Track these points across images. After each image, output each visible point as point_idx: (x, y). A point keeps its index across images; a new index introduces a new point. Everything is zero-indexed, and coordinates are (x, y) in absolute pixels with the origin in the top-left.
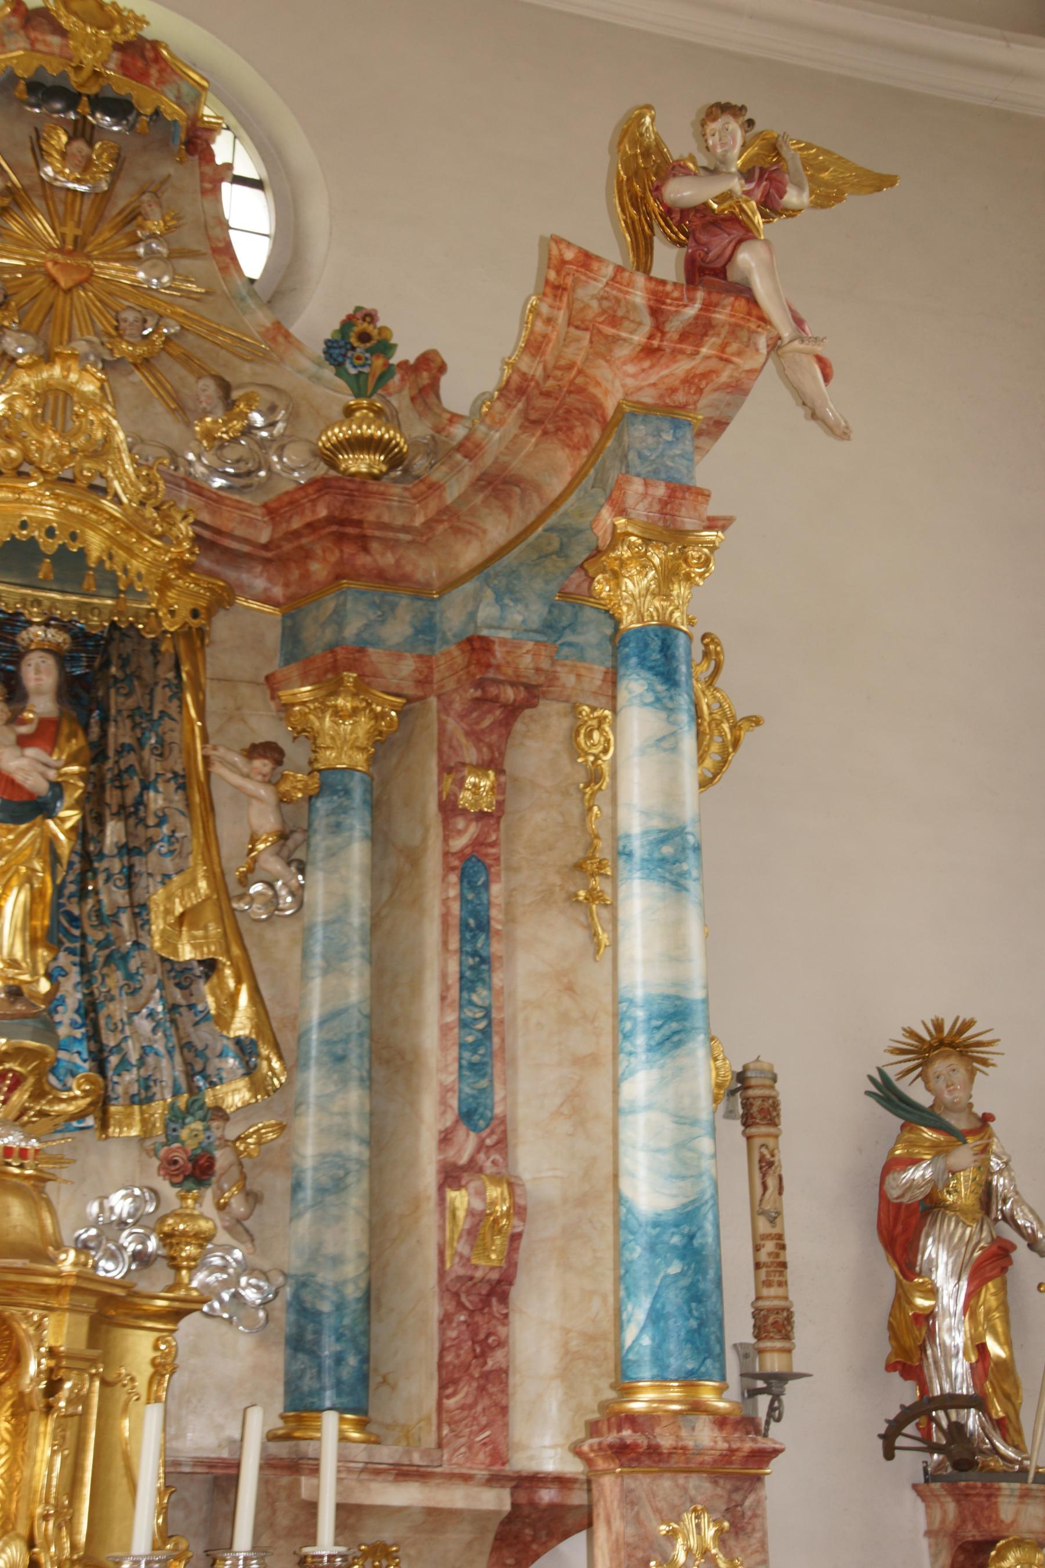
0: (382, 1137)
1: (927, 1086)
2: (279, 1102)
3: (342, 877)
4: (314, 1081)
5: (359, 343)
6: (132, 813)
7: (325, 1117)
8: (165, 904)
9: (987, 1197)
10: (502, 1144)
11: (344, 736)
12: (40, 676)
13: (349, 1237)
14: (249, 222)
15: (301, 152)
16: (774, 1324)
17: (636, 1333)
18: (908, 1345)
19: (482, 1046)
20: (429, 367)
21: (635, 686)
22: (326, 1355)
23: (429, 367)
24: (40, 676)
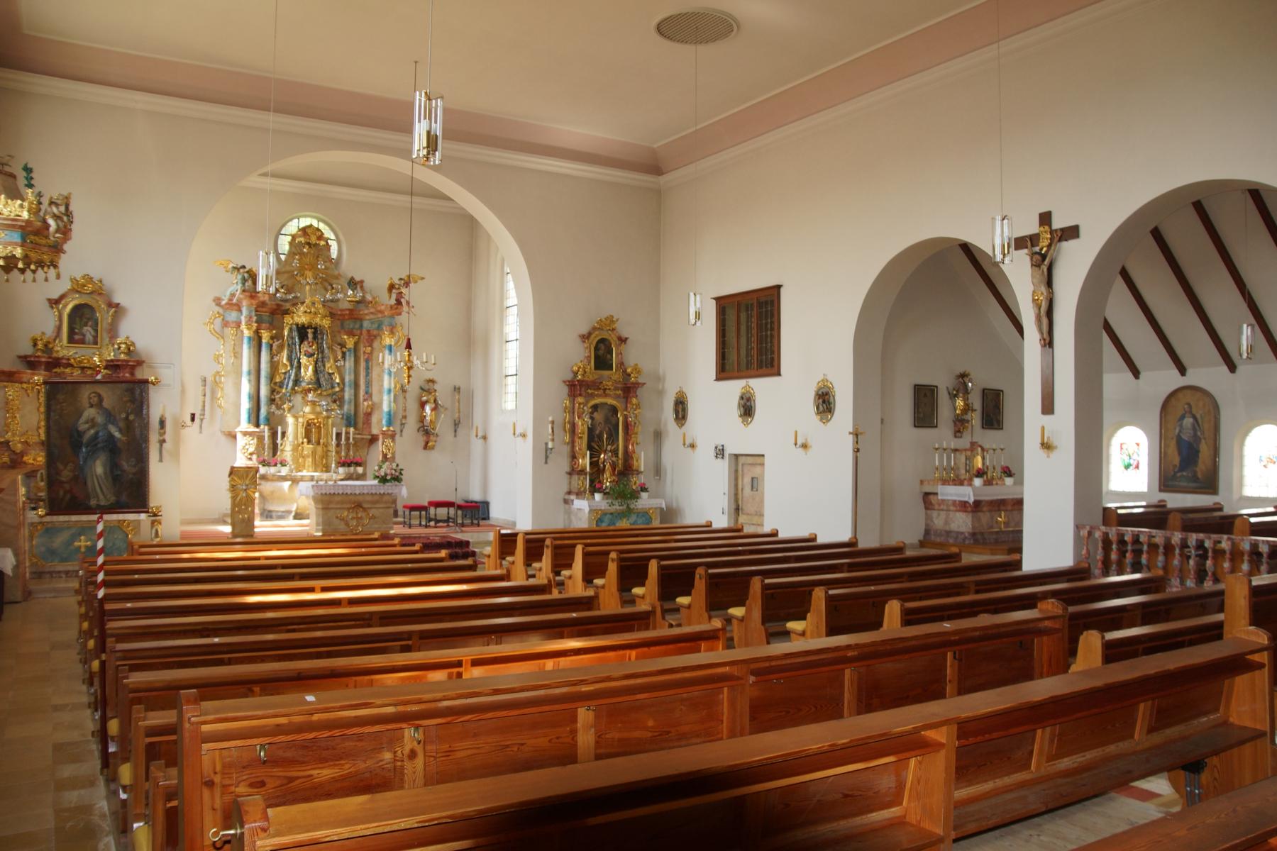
0: (356, 395)
1: (428, 388)
2: (342, 390)
3: (349, 363)
4: (347, 389)
5: (353, 284)
6: (323, 352)
7: (348, 394)
8: (328, 365)
9: (435, 400)
10: (371, 396)
11: (350, 343)
12: (310, 336)
13: (353, 408)
14: (334, 252)
15: (341, 237)
16: (405, 417)
17: (384, 422)
18: (422, 419)
19: (368, 384)
20: (362, 282)
21: (387, 352)
22: (351, 421)
23: (362, 282)
24: (310, 336)
